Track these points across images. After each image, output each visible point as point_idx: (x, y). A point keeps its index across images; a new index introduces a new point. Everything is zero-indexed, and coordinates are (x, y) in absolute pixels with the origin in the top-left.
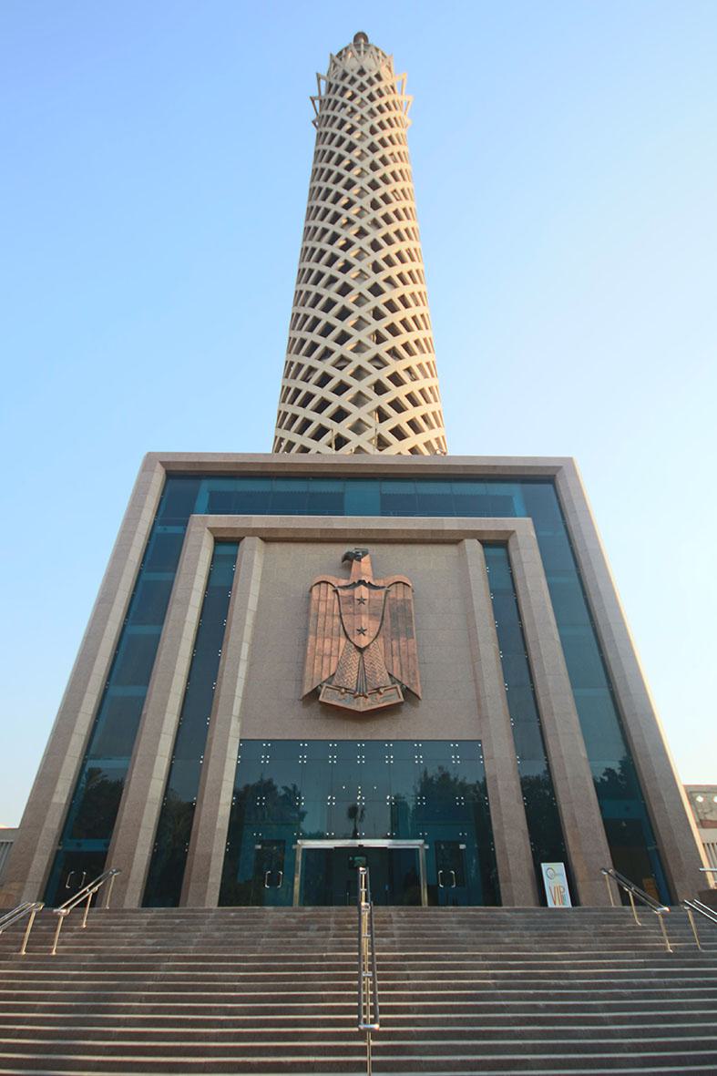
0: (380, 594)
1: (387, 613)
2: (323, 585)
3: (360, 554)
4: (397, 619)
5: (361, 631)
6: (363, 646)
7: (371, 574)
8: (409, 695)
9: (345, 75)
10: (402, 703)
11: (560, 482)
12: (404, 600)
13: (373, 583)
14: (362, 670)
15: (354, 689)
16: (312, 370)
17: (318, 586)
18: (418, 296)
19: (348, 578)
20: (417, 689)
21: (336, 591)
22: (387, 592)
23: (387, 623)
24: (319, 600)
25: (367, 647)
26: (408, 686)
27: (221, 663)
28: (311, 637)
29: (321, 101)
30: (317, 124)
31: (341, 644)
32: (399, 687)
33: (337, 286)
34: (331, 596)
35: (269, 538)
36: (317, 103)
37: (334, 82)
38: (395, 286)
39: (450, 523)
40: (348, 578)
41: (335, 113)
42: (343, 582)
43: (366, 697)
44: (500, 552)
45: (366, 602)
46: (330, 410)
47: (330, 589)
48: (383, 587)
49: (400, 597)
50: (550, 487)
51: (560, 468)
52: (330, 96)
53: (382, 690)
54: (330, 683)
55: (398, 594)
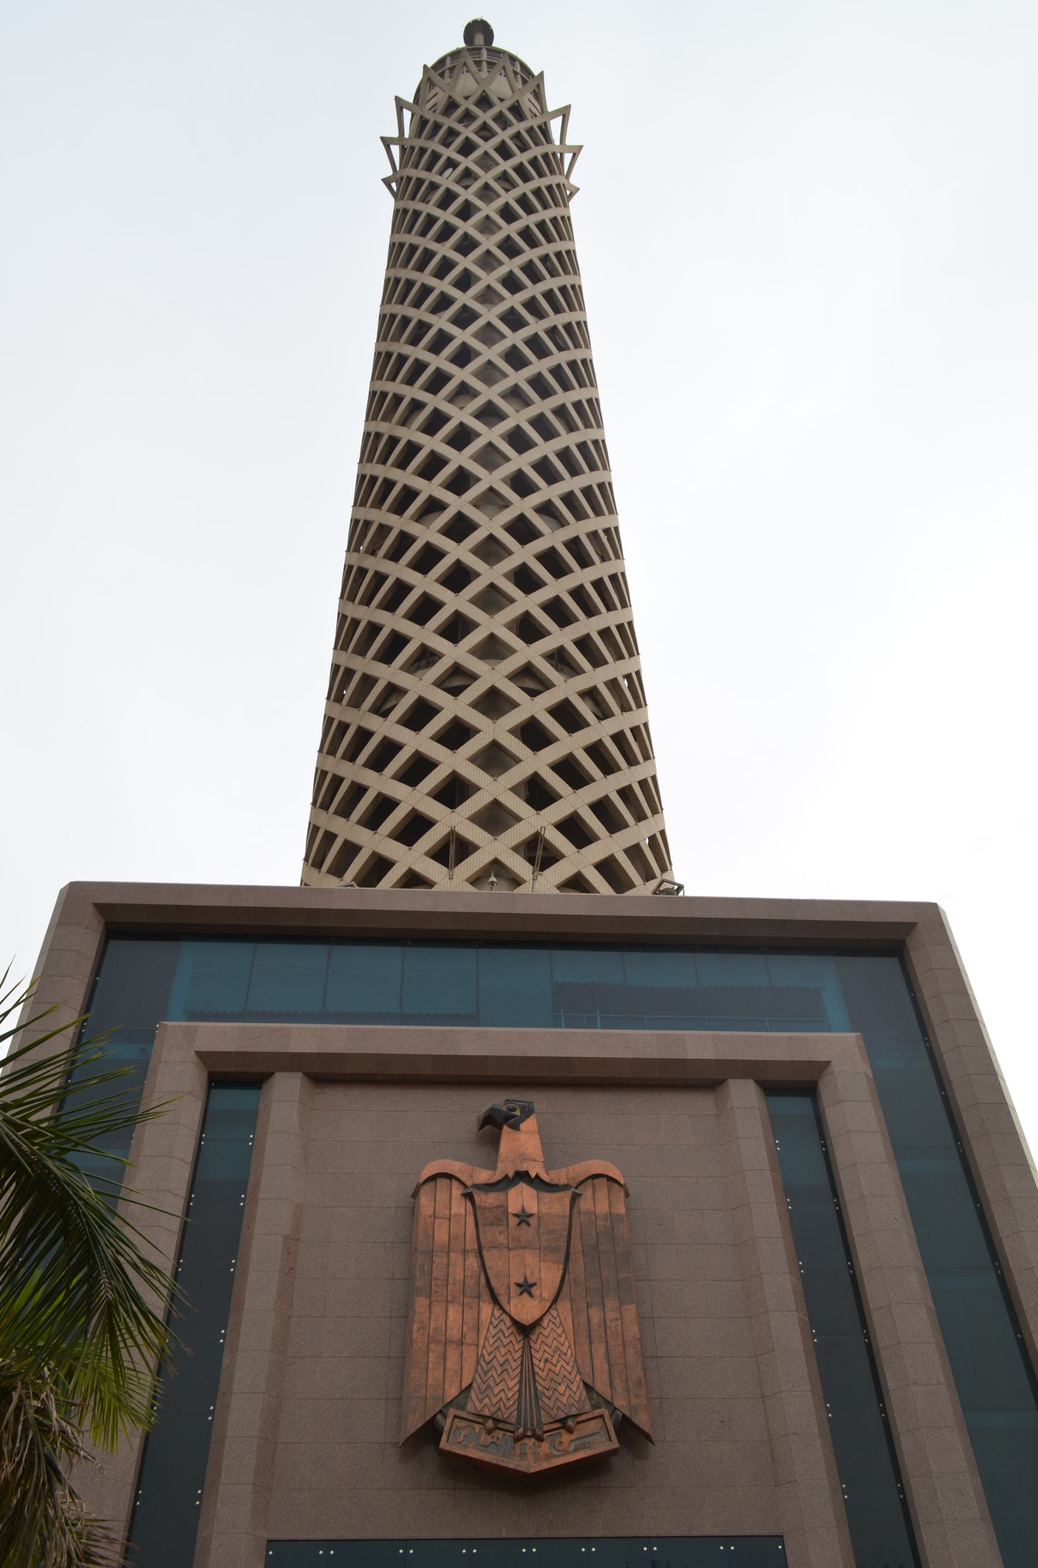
0: (557, 1205)
1: (576, 1244)
2: (442, 1182)
3: (518, 1113)
4: (601, 1260)
5: (526, 1288)
6: (527, 1319)
7: (541, 1158)
8: (628, 1431)
9: (451, 106)
10: (613, 1452)
11: (916, 957)
12: (611, 1216)
13: (544, 1176)
14: (528, 1375)
15: (513, 1420)
16: (393, 691)
17: (431, 1184)
18: (604, 538)
19: (493, 1166)
20: (642, 1420)
21: (469, 1197)
22: (575, 1197)
23: (578, 1267)
24: (434, 1215)
25: (538, 1323)
26: (627, 1413)
27: (226, 1361)
28: (421, 1302)
29: (403, 150)
30: (394, 185)
31: (483, 1316)
32: (606, 1413)
33: (443, 519)
34: (459, 1207)
35: (327, 1073)
36: (395, 150)
37: (432, 117)
38: (562, 523)
39: (699, 1044)
40: (493, 1166)
41: (433, 177)
42: (484, 1176)
43: (540, 1439)
44: (799, 1106)
45: (533, 1221)
46: (433, 780)
47: (457, 1191)
48: (566, 1187)
49: (602, 1207)
50: (890, 965)
51: (912, 926)
52: (418, 143)
53: (570, 1423)
54: (463, 1408)
55: (598, 1202)
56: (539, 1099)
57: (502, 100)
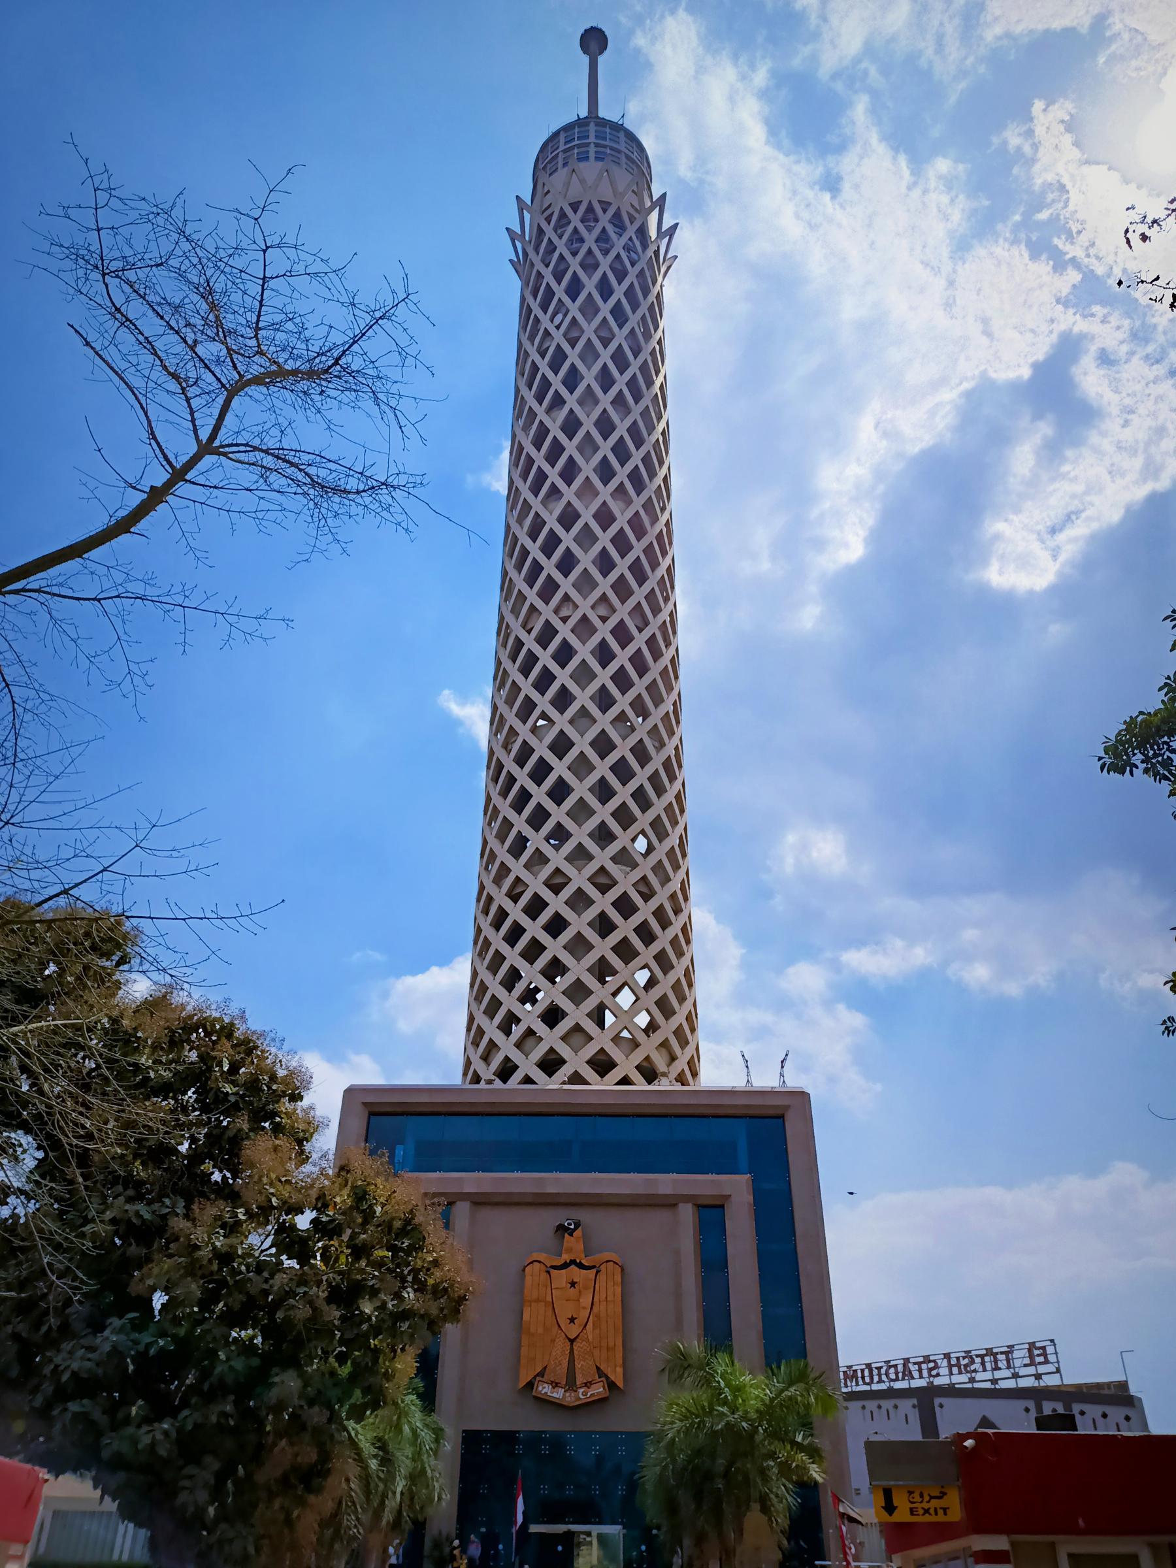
35: (480, 1201)
56: (584, 1215)
57: (605, 206)
